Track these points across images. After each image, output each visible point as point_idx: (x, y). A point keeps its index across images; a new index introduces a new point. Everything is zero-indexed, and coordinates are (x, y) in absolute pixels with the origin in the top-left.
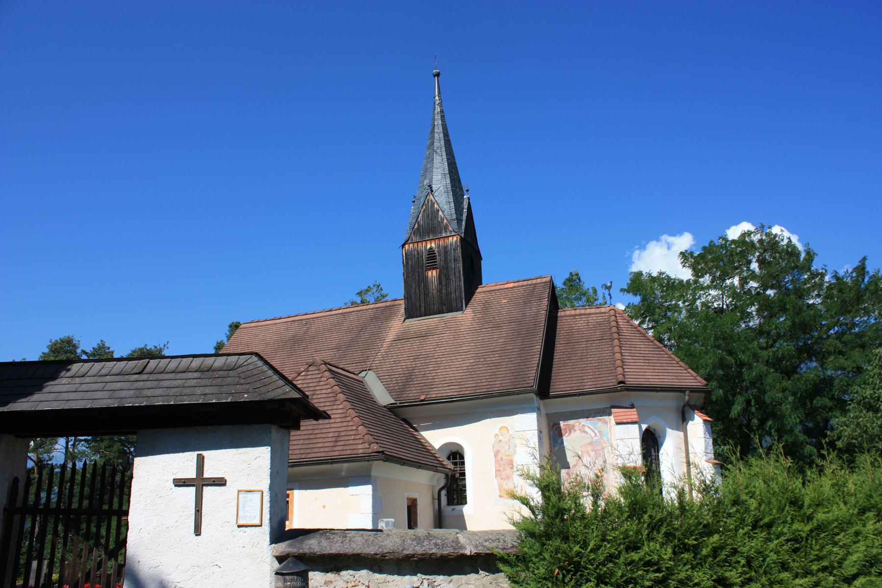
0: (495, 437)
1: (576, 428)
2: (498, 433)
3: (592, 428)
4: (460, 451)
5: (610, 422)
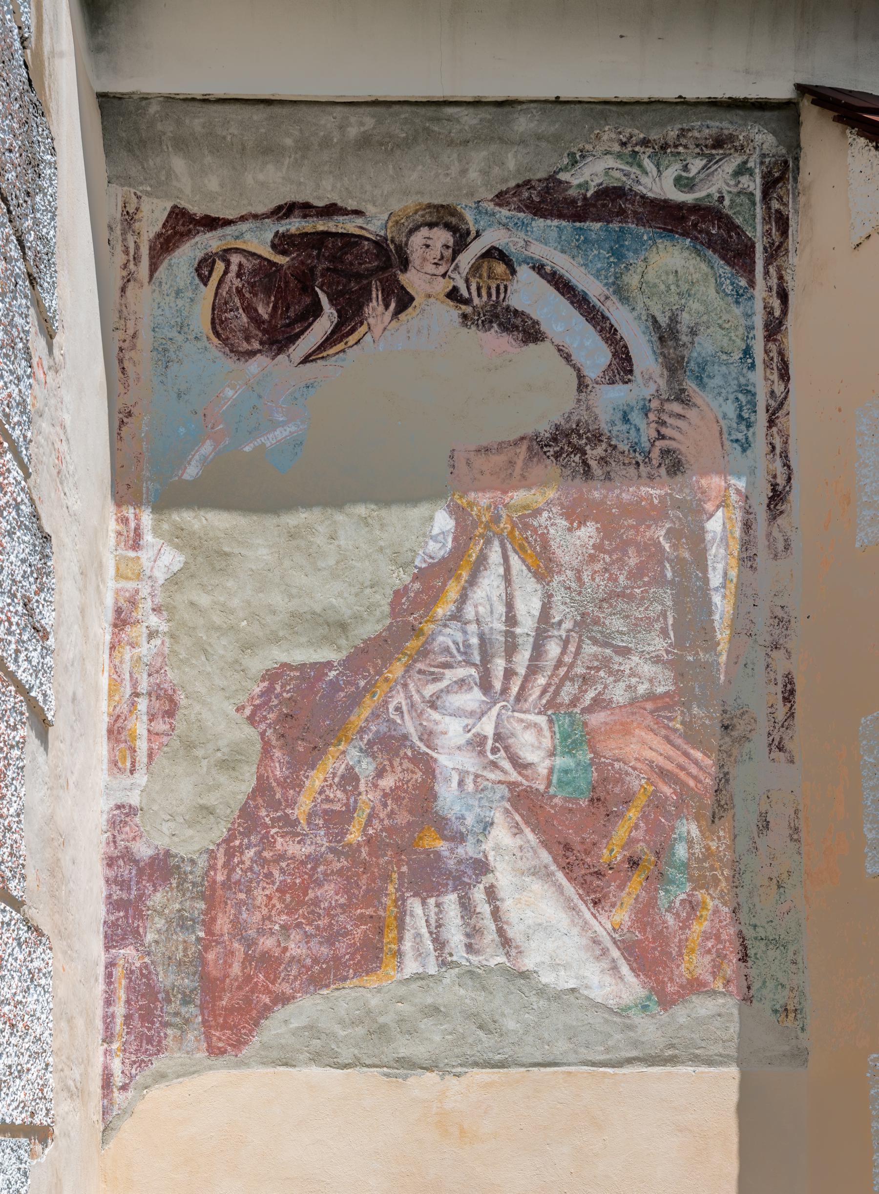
5: (775, 252)
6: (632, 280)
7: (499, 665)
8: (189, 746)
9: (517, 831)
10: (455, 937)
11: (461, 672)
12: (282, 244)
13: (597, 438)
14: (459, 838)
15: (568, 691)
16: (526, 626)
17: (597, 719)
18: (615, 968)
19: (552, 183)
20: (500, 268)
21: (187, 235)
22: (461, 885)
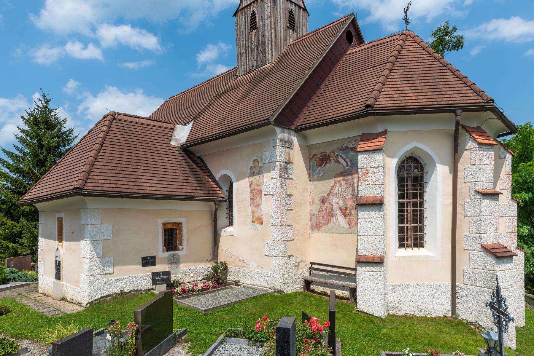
1: (331, 158)
3: (344, 157)
4: (427, 168)
6: (348, 156)
7: (338, 195)
9: (339, 211)
10: (335, 221)
11: (335, 196)
12: (321, 156)
13: (345, 172)
16: (340, 191)
17: (346, 200)
22: (335, 216)
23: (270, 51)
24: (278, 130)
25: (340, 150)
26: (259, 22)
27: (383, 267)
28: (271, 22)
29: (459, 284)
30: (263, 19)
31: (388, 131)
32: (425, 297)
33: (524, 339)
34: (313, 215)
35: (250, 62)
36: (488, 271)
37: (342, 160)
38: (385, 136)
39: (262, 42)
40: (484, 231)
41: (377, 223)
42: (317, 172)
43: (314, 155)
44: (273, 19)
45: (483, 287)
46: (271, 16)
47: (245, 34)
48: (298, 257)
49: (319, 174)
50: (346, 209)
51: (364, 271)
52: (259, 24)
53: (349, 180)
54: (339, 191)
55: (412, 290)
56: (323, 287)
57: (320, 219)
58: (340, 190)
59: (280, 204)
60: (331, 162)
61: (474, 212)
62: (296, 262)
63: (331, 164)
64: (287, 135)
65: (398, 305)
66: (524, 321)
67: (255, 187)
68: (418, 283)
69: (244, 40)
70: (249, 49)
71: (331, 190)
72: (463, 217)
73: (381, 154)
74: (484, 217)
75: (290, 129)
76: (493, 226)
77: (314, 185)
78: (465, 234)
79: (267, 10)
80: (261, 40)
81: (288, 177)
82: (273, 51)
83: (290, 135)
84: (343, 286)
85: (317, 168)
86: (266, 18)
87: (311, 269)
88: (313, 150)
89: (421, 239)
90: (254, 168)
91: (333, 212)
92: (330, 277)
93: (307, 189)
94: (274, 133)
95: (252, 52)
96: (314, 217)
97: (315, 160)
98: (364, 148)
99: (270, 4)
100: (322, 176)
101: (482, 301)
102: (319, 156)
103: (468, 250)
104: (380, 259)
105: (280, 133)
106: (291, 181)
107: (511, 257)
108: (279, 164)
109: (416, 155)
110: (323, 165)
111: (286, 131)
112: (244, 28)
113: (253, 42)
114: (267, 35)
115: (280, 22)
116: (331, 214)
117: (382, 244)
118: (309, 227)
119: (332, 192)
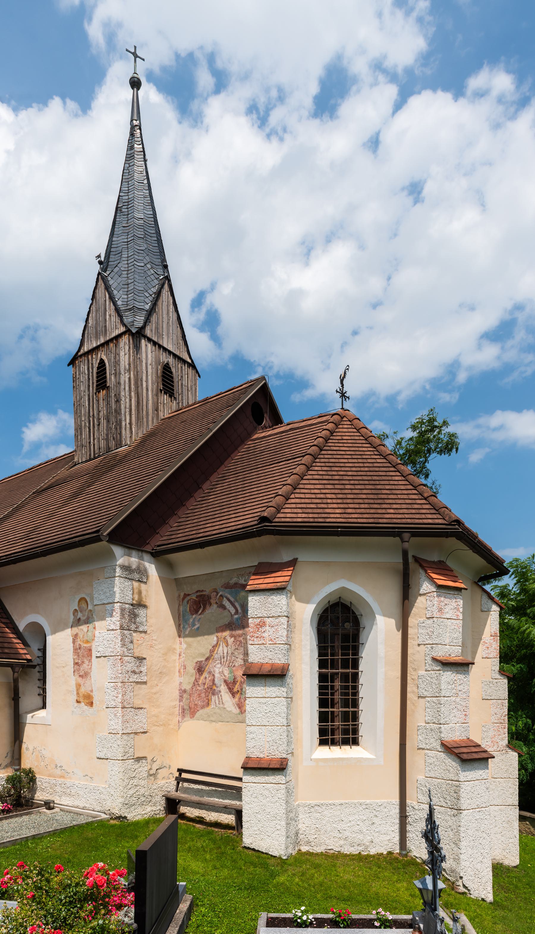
0: (74, 614)
1: (212, 601)
2: (77, 608)
3: (232, 599)
7: (223, 660)
8: (187, 673)
12: (197, 597)
14: (217, 687)
15: (231, 664)
16: (225, 654)
17: (234, 668)
18: (236, 708)
19: (228, 583)
20: (222, 598)
21: (186, 597)
23: (128, 426)
24: (117, 551)
25: (226, 588)
26: (110, 378)
27: (285, 777)
28: (130, 378)
29: (411, 802)
30: (117, 374)
31: (298, 560)
32: (358, 823)
33: (513, 884)
34: (185, 691)
35: (96, 441)
36: (450, 782)
37: (229, 604)
38: (292, 568)
39: (116, 411)
40: (445, 719)
41: (276, 705)
42: (190, 623)
43: (186, 595)
44: (134, 375)
45: (444, 807)
46: (129, 371)
47: (89, 395)
48: (155, 760)
49: (194, 625)
50: (234, 682)
51: (255, 783)
52: (111, 380)
53: (239, 636)
54: (223, 654)
55: (338, 813)
56: (199, 809)
57: (195, 698)
58: (225, 652)
59: (120, 672)
60: (212, 607)
61: (431, 690)
62: (151, 769)
63: (212, 610)
64: (137, 560)
65: (316, 836)
66: (518, 857)
67: (82, 644)
68: (347, 801)
69: (87, 406)
70: (94, 421)
71: (212, 651)
72: (416, 698)
73: (284, 596)
74: (445, 698)
75: (142, 551)
76: (460, 712)
77: (186, 643)
78: (419, 724)
79: (124, 359)
80: (114, 407)
81: (136, 628)
82: (133, 426)
83: (143, 560)
84: (226, 807)
85: (190, 616)
86: (123, 373)
87: (179, 780)
88: (185, 586)
89: (355, 731)
90: (79, 613)
91: (214, 688)
92: (210, 794)
93: (175, 649)
94: (112, 556)
95: (99, 425)
96: (185, 696)
97: (188, 602)
98: (258, 586)
99: (129, 351)
100: (198, 628)
101: (442, 828)
102: (194, 597)
103: (423, 749)
104: (280, 762)
105: (122, 557)
106: (143, 635)
107: (486, 759)
108: (120, 606)
109: (347, 599)
110: (200, 611)
111: (134, 553)
112: (87, 386)
113: (100, 409)
114: (123, 399)
115: (147, 381)
116: (212, 690)
117: (284, 740)
118: (177, 711)
119: (214, 655)
